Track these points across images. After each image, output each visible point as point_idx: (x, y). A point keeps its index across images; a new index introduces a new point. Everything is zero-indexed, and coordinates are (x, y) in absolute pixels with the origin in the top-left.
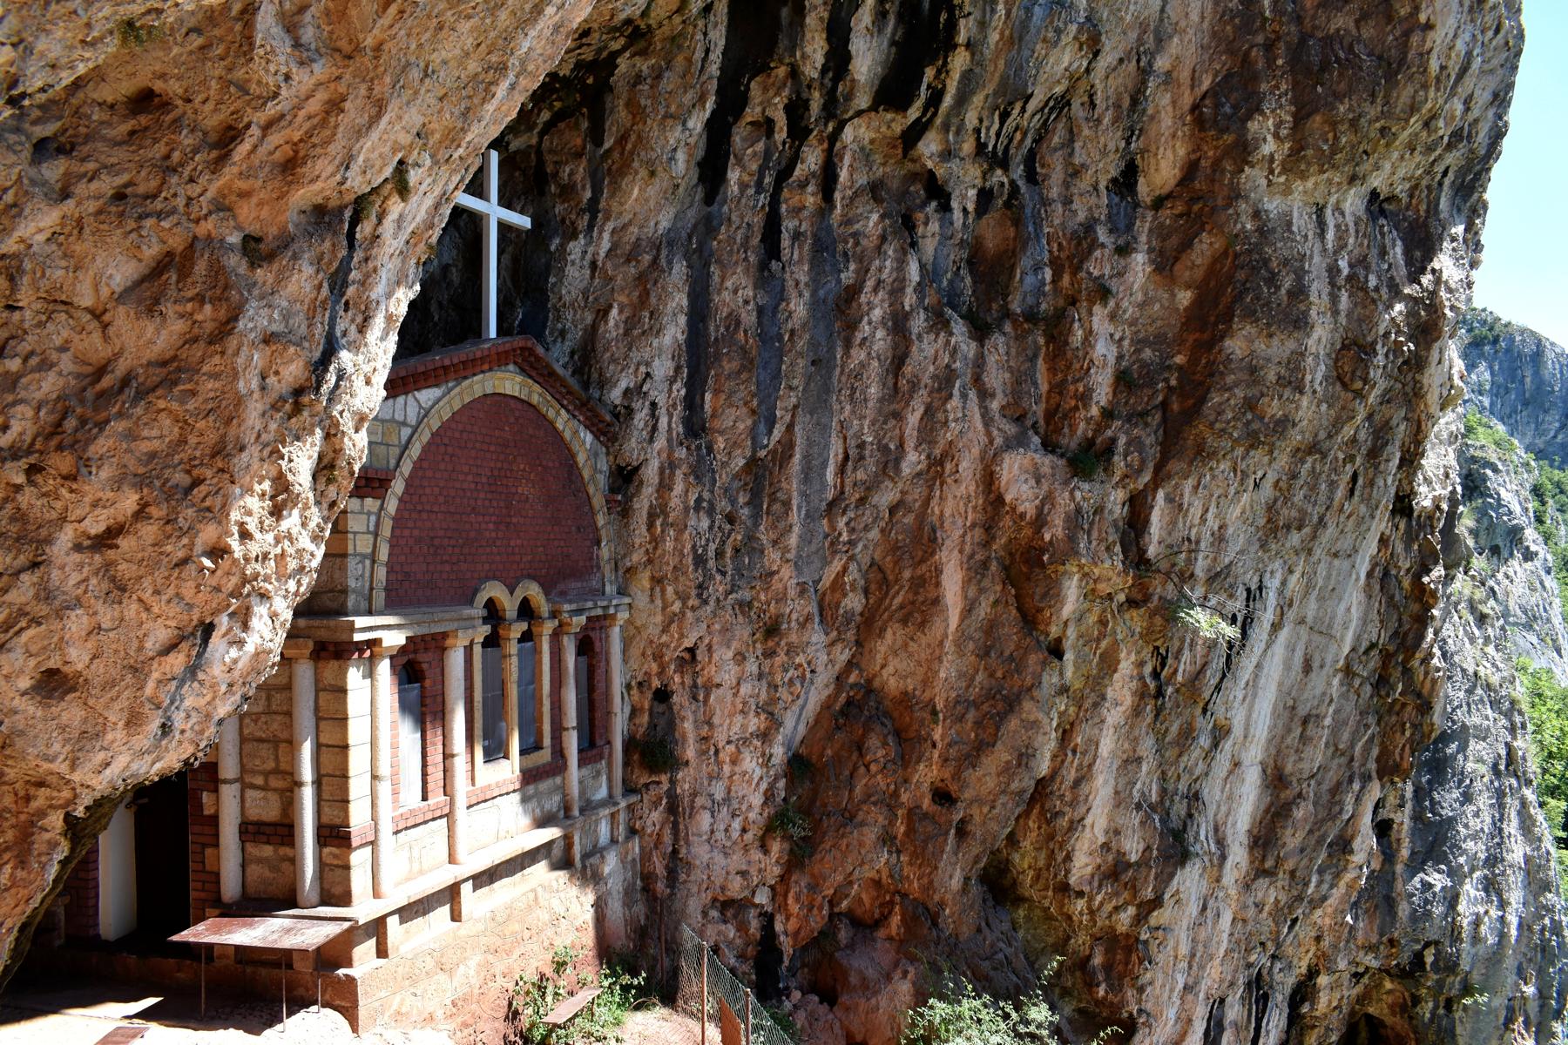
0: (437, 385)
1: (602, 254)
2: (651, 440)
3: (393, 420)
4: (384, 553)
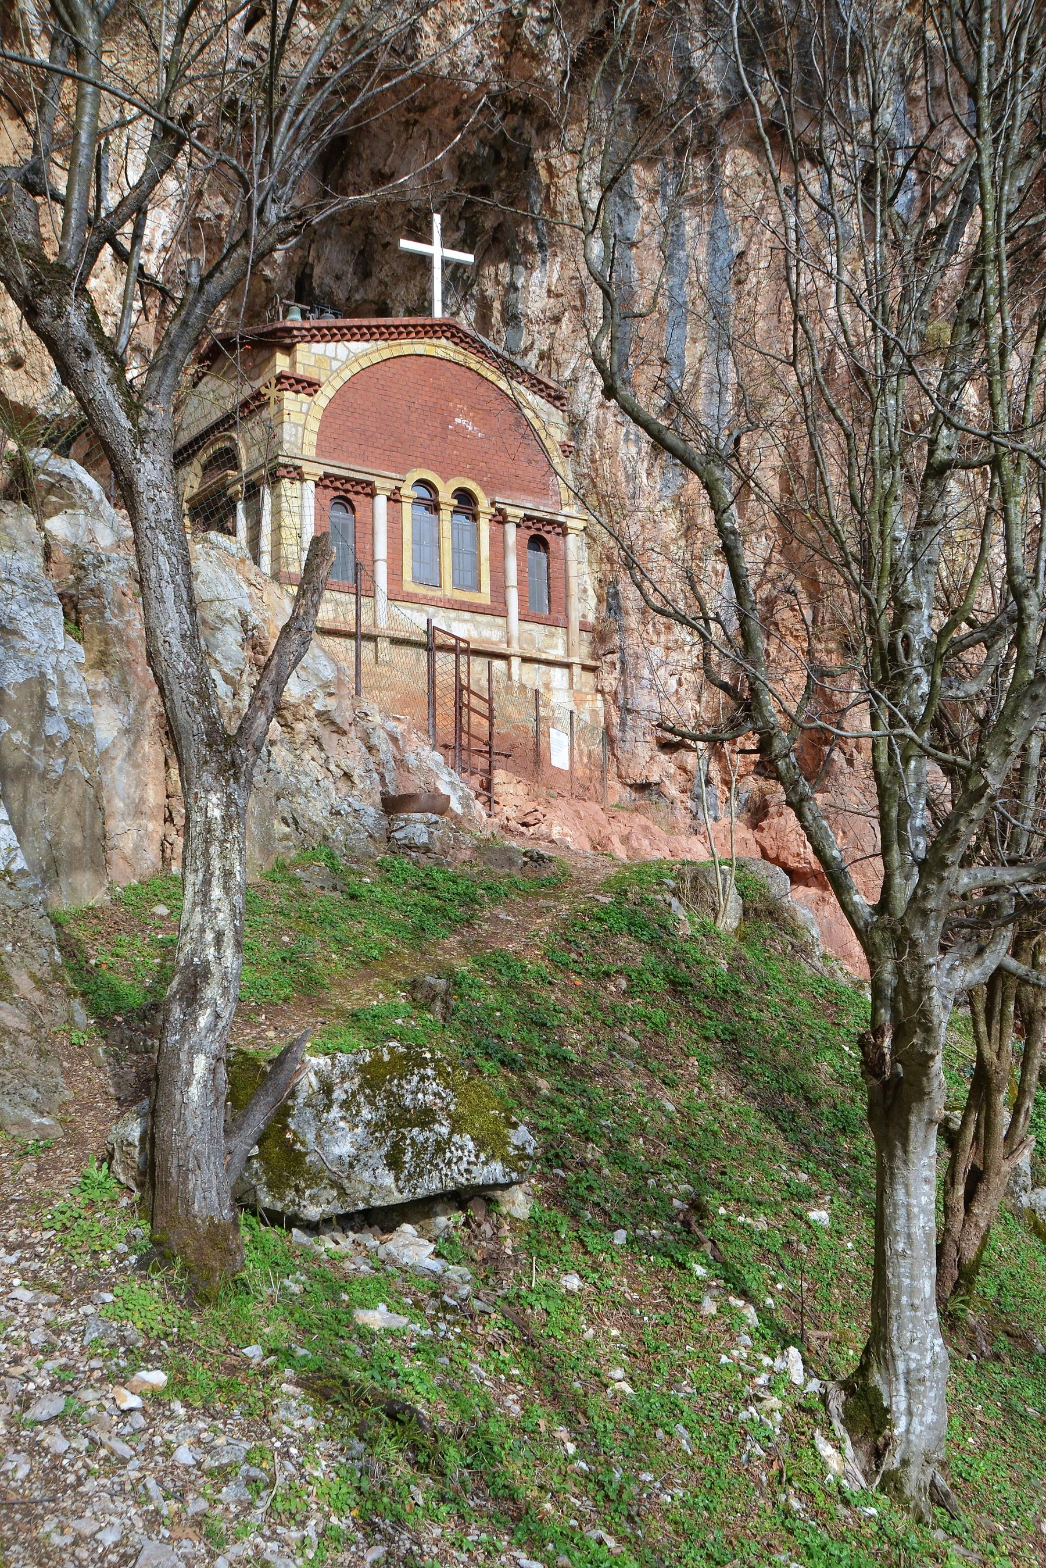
0: (367, 341)
1: (554, 281)
2: (590, 398)
3: (325, 355)
4: (315, 426)
